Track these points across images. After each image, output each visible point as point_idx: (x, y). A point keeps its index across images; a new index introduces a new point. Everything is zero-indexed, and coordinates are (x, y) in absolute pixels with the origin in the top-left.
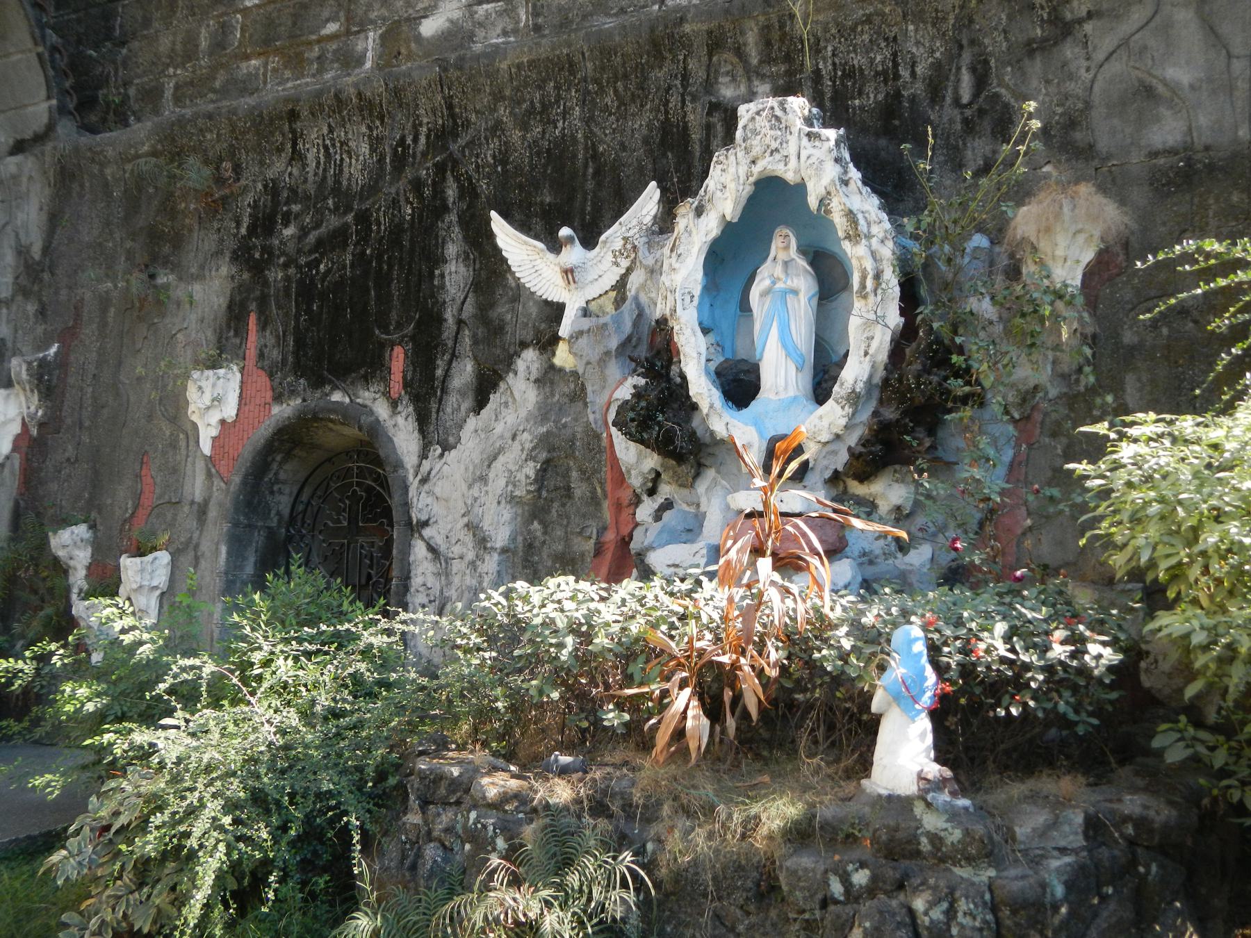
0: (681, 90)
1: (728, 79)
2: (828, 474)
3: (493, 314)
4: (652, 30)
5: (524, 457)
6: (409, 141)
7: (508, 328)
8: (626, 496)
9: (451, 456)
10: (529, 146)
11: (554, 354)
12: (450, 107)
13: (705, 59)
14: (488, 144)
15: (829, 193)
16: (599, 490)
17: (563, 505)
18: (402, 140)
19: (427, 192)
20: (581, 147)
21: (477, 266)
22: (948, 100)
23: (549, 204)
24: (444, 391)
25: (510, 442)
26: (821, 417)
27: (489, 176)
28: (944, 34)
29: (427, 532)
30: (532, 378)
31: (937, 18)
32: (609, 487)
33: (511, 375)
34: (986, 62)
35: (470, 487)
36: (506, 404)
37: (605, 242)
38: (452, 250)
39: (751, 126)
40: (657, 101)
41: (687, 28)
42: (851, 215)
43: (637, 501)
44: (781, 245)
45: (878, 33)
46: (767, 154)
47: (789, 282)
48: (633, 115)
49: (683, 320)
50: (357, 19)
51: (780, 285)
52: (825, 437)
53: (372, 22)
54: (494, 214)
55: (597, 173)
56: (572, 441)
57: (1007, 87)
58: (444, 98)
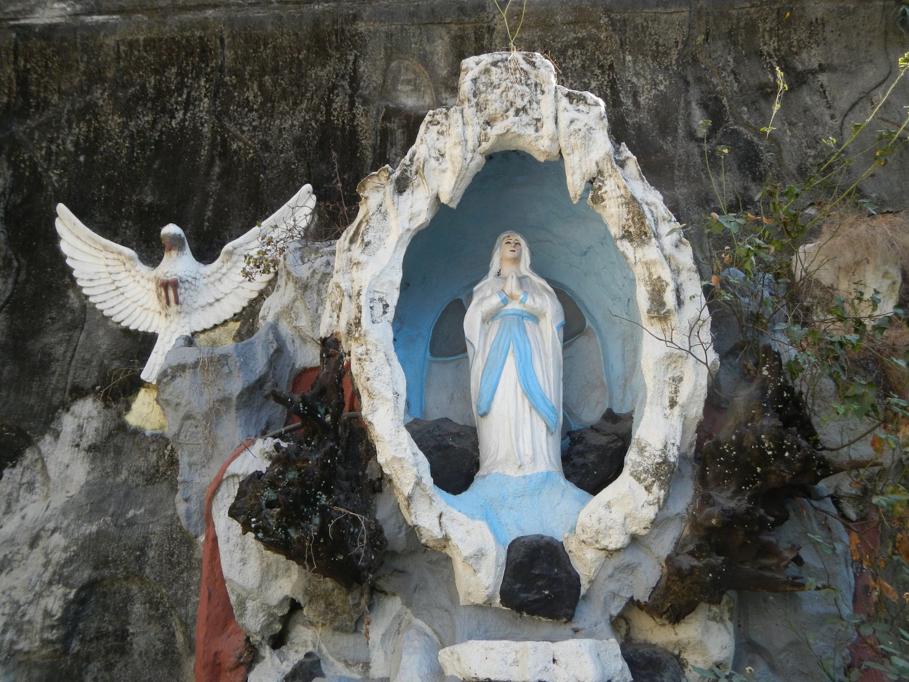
0: (349, 91)
1: (409, 88)
3: (35, 346)
4: (317, 23)
5: (46, 577)
7: (56, 367)
8: (231, 648)
10: (131, 136)
11: (128, 408)
13: (381, 63)
14: (70, 128)
15: (600, 172)
16: (180, 638)
17: (109, 667)
20: (206, 143)
21: (23, 277)
22: (681, 132)
23: (151, 205)
25: (25, 549)
26: (608, 506)
27: (64, 166)
28: (667, 68)
30: (85, 444)
31: (658, 52)
32: (199, 633)
33: (48, 438)
34: (717, 100)
36: (30, 487)
37: (230, 253)
39: (483, 79)
40: (316, 101)
41: (361, 27)
42: (632, 202)
43: (252, 657)
44: (510, 255)
45: (592, 60)
46: (511, 112)
47: (529, 302)
48: (281, 113)
49: (371, 338)
52: (616, 540)
54: (61, 208)
55: (226, 173)
56: (142, 549)
57: (747, 125)
58: (16, 70)
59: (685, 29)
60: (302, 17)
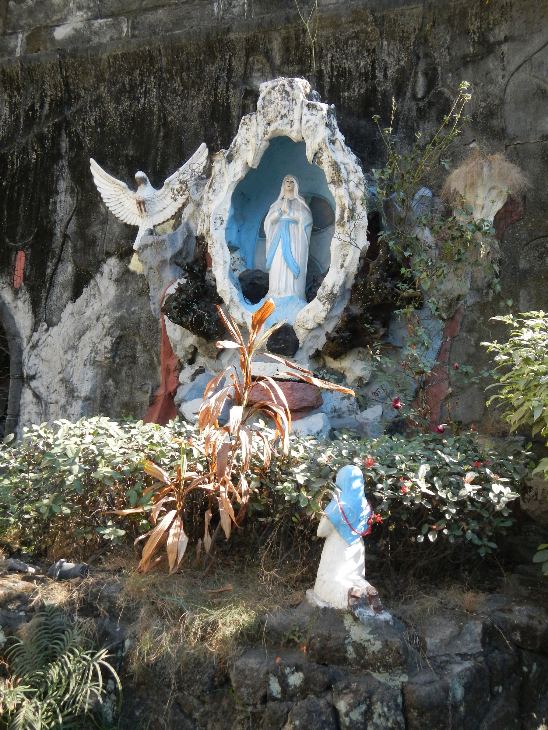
0: (226, 80)
1: (259, 74)
2: (312, 352)
3: (89, 232)
4: (208, 36)
5: (104, 333)
6: (37, 107)
7: (99, 242)
8: (173, 363)
9: (54, 330)
10: (120, 115)
11: (129, 262)
12: (67, 84)
13: (244, 59)
14: (91, 112)
15: (321, 149)
16: (155, 359)
17: (130, 369)
18: (32, 107)
19: (47, 144)
20: (156, 117)
21: (80, 198)
22: (408, 94)
23: (132, 156)
24: (52, 284)
25: (95, 322)
26: (308, 311)
27: (91, 135)
28: (407, 49)
29: (33, 384)
30: (113, 278)
31: (403, 37)
32: (162, 357)
33: (99, 275)
34: (435, 69)
35: (65, 353)
36: (94, 296)
37: (168, 184)
38: (62, 185)
39: (268, 98)
40: (209, 87)
41: (232, 36)
42: (335, 165)
43: (181, 368)
44: (288, 188)
45: (363, 46)
46: (279, 118)
47: (292, 215)
48: (192, 96)
49: (214, 237)
50: (11, 25)
51: (285, 217)
52: (311, 325)
53: (22, 27)
54: (92, 161)
55: (166, 136)
56: (139, 323)
57: (449, 87)
58: (62, 77)
59: (420, 20)
60: (200, 32)
